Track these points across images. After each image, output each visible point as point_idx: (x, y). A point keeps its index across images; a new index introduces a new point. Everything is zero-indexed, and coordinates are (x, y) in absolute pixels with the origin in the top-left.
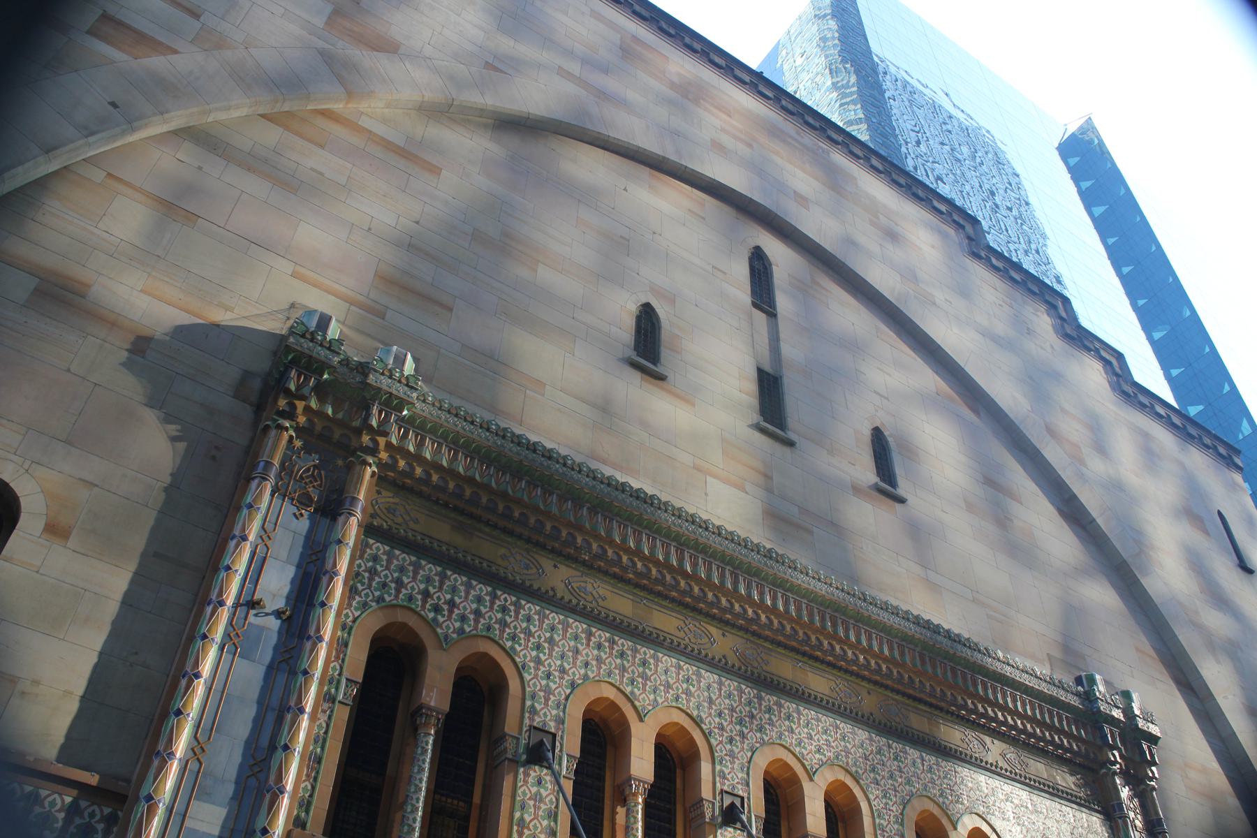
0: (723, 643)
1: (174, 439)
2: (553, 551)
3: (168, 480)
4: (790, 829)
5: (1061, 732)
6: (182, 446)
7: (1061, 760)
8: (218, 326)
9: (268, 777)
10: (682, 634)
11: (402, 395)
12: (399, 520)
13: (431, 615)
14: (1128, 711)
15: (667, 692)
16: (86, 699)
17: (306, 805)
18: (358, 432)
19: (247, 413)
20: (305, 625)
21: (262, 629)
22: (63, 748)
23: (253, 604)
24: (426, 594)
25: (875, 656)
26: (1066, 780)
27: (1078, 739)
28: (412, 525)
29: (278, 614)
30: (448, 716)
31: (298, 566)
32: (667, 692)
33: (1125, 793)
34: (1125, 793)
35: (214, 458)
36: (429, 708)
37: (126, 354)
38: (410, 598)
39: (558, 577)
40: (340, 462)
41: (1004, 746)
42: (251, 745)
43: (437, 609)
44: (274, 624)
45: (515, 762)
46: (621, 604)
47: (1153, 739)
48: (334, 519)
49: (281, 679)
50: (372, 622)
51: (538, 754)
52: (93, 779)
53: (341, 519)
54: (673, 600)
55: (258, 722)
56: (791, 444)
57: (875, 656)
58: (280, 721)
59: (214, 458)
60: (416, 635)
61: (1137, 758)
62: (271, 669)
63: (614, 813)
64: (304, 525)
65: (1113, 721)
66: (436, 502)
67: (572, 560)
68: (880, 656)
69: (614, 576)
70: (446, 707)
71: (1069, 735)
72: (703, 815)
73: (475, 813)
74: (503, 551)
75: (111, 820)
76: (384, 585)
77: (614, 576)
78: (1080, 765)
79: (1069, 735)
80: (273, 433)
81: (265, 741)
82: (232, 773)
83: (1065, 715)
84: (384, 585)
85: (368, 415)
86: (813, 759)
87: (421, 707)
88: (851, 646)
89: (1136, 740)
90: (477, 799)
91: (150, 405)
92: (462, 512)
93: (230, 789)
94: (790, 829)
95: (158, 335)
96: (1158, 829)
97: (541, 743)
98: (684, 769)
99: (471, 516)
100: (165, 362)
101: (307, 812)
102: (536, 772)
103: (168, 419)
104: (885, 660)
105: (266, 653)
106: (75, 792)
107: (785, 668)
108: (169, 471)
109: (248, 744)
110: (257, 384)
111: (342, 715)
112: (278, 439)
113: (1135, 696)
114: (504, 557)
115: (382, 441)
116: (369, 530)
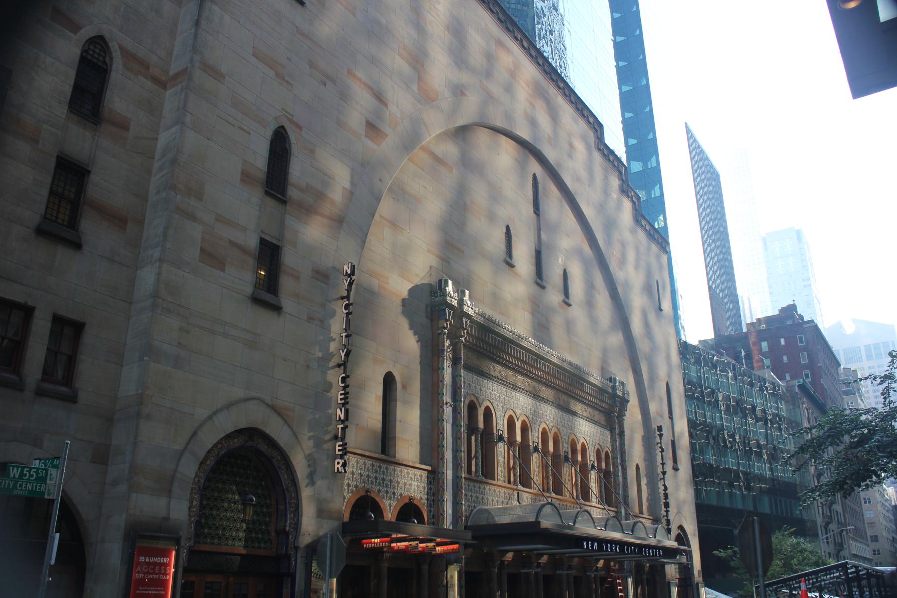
26: (597, 416)
39: (497, 370)
50: (467, 402)
52: (429, 468)
56: (543, 287)
91: (410, 329)
103: (415, 334)
110: (429, 309)
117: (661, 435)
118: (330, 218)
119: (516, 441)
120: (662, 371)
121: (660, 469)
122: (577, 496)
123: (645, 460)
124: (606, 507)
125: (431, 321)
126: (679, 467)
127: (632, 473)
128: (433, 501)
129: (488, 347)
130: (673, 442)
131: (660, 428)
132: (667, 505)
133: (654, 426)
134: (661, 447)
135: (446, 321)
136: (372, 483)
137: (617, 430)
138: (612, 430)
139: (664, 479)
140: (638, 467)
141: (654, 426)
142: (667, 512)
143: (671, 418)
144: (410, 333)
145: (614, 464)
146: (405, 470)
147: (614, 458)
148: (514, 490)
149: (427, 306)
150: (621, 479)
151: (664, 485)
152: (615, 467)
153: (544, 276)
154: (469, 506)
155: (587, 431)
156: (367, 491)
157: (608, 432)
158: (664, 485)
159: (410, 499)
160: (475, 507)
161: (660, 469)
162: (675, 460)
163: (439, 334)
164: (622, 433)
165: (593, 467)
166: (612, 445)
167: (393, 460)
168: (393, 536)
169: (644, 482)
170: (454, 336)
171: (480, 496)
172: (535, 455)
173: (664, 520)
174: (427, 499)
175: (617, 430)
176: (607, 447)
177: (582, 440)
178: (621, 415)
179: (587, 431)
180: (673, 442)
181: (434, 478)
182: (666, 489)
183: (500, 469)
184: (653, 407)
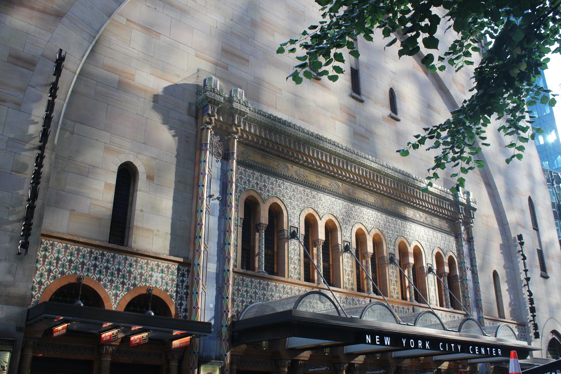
0: (341, 187)
1: (174, 136)
2: (291, 161)
3: (176, 152)
4: (361, 250)
5: (445, 209)
6: (177, 138)
7: (444, 218)
8: (177, 85)
9: (225, 253)
10: (330, 186)
11: (244, 111)
12: (245, 156)
13: (259, 191)
14: (468, 201)
15: (328, 207)
16: (171, 234)
17: (236, 261)
18: (231, 126)
19: (193, 120)
20: (226, 201)
21: (214, 204)
22: (170, 250)
23: (210, 196)
24: (257, 184)
25: (389, 188)
27: (451, 211)
28: (249, 158)
29: (218, 198)
30: (268, 225)
31: (220, 180)
32: (328, 207)
33: (463, 228)
34: (463, 228)
35: (187, 141)
36: (263, 224)
37: (152, 103)
38: (253, 186)
39: (293, 170)
40: (226, 138)
41: (427, 215)
42: (219, 243)
43: (261, 189)
44: (217, 202)
45: (288, 239)
46: (313, 178)
47: (475, 209)
48: (228, 161)
49: (223, 220)
50: (244, 196)
51: (294, 235)
52: (181, 260)
53: (230, 161)
54: (328, 174)
55: (219, 236)
56: (362, 101)
57: (389, 188)
58: (225, 234)
59: (187, 141)
60: (256, 199)
61: (468, 216)
62: (220, 218)
63: (313, 250)
64: (219, 164)
65: (462, 204)
66: (256, 148)
67: (297, 164)
68: (391, 188)
69: (310, 168)
70: (267, 223)
71: (448, 210)
72: (339, 249)
73: (275, 255)
74: (276, 163)
75: (188, 271)
76: (245, 182)
77: (310, 168)
78: (450, 220)
79: (448, 210)
80: (205, 131)
81: (222, 242)
82: (216, 253)
83: (447, 203)
84: (245, 182)
85: (234, 120)
86: (369, 227)
87: (260, 223)
88: (382, 185)
89: (469, 209)
90: (275, 250)
91: (164, 124)
92: (263, 150)
93: (216, 258)
94: (361, 250)
95: (161, 94)
96: (471, 240)
97: (294, 231)
98: (331, 233)
99: (266, 152)
100: (164, 102)
101: (236, 262)
102: (294, 241)
103: (171, 128)
104: (392, 189)
105: (217, 213)
106: (178, 264)
107: (362, 195)
108: (175, 149)
109: (218, 243)
110: (194, 108)
111: (240, 229)
112: (207, 132)
113: (471, 194)
114: (277, 165)
115: (239, 128)
116: (238, 163)
117: (522, 244)
118: (43, 12)
119: (367, 253)
120: (523, 186)
121: (523, 276)
122: (411, 297)
123: (505, 267)
124: (451, 309)
125: (197, 118)
126: (549, 274)
127: (485, 279)
128: (187, 294)
129: (280, 147)
130: (540, 252)
131: (520, 237)
132: (533, 310)
133: (514, 235)
134: (523, 255)
135: (236, 126)
136: (88, 270)
137: (464, 236)
138: (457, 236)
139: (528, 285)
140: (495, 274)
141: (514, 235)
142: (534, 316)
143: (536, 227)
144: (165, 128)
145: (460, 268)
146: (153, 263)
147: (461, 263)
148: (365, 297)
149: (190, 104)
150: (470, 284)
151: (529, 291)
152: (462, 270)
153: (363, 91)
154: (243, 302)
155: (424, 237)
156: (79, 279)
157: (452, 239)
158: (529, 291)
159: (149, 290)
160: (251, 303)
161: (523, 276)
162: (543, 268)
163: (203, 129)
164: (470, 240)
165: (430, 270)
166: (458, 251)
167: (129, 250)
168: (133, 329)
169: (504, 287)
170: (224, 133)
171: (260, 293)
172: (346, 255)
173: (530, 325)
174: (177, 292)
175: (464, 236)
176: (452, 251)
177: (414, 244)
178: (468, 223)
179: (424, 237)
180: (540, 252)
181: (187, 269)
182: (531, 294)
183: (292, 266)
184: (511, 217)
